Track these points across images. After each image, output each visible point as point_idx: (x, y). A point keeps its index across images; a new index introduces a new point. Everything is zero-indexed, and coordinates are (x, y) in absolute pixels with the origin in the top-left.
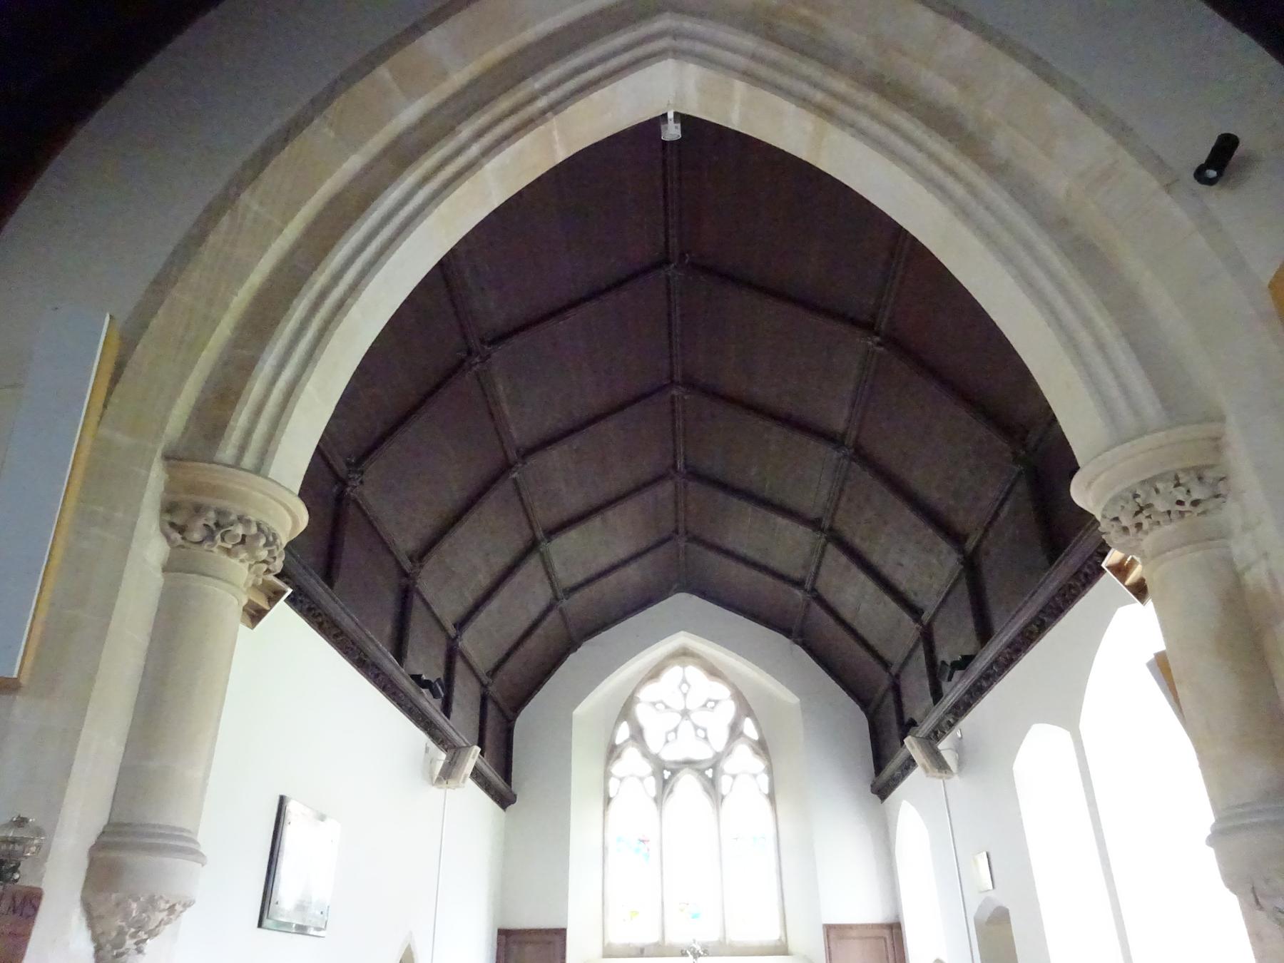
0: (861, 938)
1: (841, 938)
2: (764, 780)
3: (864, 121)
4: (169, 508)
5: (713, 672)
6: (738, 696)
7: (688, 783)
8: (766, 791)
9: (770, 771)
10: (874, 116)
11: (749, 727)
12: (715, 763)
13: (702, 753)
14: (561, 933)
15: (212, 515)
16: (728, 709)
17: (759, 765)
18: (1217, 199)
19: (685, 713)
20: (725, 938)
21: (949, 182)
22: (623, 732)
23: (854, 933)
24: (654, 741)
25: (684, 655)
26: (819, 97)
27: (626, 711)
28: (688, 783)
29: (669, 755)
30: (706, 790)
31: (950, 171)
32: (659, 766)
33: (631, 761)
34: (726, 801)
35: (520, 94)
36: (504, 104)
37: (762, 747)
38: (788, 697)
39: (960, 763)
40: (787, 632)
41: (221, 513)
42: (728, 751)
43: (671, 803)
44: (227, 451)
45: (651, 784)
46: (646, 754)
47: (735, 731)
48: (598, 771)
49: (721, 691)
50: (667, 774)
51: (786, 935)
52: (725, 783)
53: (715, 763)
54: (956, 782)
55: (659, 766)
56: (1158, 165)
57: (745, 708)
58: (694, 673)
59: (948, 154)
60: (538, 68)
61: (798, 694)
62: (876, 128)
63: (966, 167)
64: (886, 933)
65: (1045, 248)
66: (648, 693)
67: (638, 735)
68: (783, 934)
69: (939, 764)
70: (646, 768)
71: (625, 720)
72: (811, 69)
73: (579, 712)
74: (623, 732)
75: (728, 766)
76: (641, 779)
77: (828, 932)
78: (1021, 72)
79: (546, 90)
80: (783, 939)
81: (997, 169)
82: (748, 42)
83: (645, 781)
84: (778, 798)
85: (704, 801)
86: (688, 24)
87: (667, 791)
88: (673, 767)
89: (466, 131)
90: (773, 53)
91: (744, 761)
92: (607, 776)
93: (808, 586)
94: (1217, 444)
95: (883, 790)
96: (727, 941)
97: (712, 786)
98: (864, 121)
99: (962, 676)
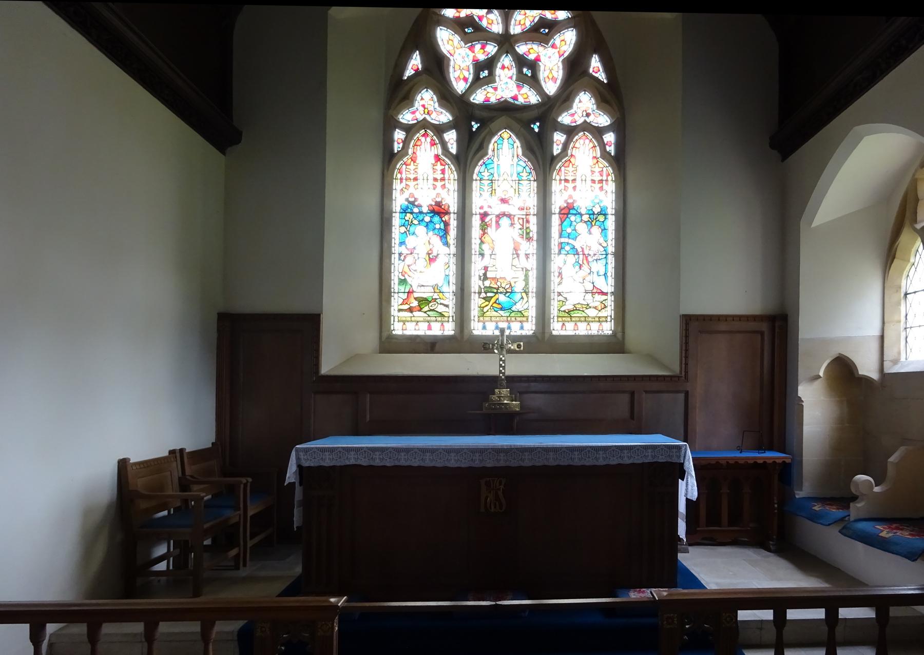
9: (619, 127)
13: (529, 97)
17: (602, 120)
20: (543, 333)
42: (564, 98)
46: (446, 96)
48: (375, 115)
50: (475, 126)
51: (623, 332)
52: (559, 138)
68: (620, 329)
74: (415, 62)
75: (565, 119)
80: (619, 335)
87: (475, 147)
88: (485, 114)
92: (391, 124)
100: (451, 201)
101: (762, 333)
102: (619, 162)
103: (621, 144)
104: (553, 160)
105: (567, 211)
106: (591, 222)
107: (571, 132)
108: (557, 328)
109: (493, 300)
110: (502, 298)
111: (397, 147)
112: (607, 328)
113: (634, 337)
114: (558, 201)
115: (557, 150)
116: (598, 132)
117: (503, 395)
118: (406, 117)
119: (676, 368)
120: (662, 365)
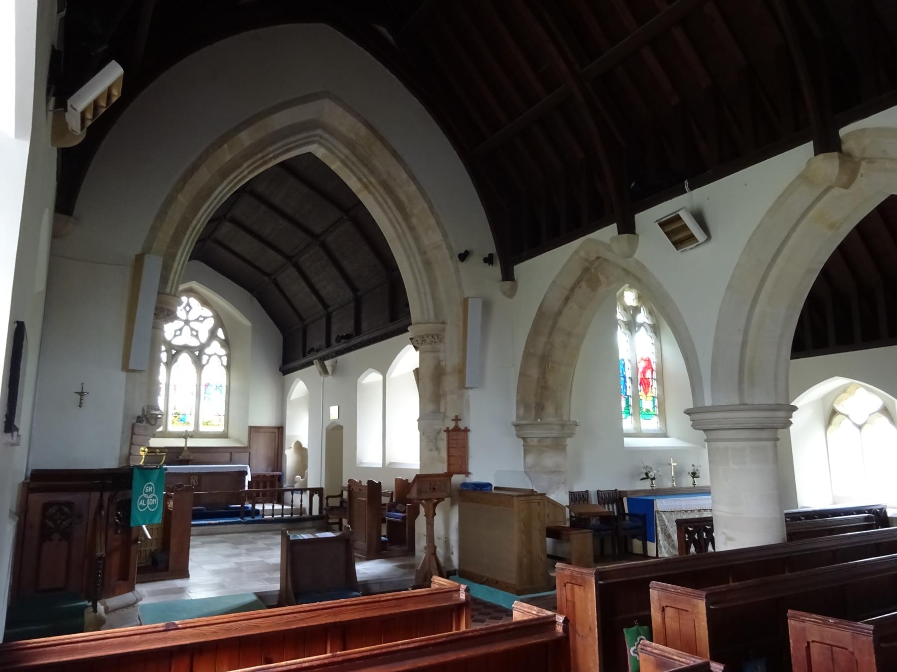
2: (225, 360)
3: (377, 195)
5: (205, 302)
7: (184, 358)
8: (225, 364)
9: (229, 356)
10: (381, 195)
11: (220, 333)
12: (202, 348)
13: (194, 343)
16: (210, 323)
17: (223, 352)
18: (462, 265)
19: (187, 322)
21: (397, 226)
23: (262, 430)
26: (365, 180)
29: (177, 342)
31: (399, 224)
34: (205, 368)
36: (260, 155)
37: (226, 344)
39: (334, 371)
40: (250, 290)
41: (168, 310)
44: (168, 290)
47: (213, 335)
49: (207, 312)
52: (205, 359)
53: (202, 348)
54: (329, 379)
56: (450, 248)
57: (220, 322)
58: (194, 302)
59: (400, 219)
60: (273, 143)
61: (251, 322)
62: (380, 199)
63: (404, 225)
64: (276, 431)
65: (418, 258)
69: (325, 371)
72: (365, 171)
75: (208, 351)
77: (250, 429)
78: (425, 205)
79: (273, 151)
81: (412, 229)
82: (346, 151)
85: (192, 368)
86: (326, 136)
88: (178, 349)
89: (245, 165)
90: (354, 159)
91: (216, 348)
94: (443, 330)
96: (167, 432)
97: (198, 362)
98: (377, 195)
99: (345, 343)
101: (275, 433)
102: (228, 368)
103: (229, 362)
104: (204, 366)
105: (207, 385)
106: (216, 389)
107: (210, 356)
109: (178, 417)
110: (181, 416)
113: (232, 432)
115: (204, 361)
116: (220, 357)
120: (243, 444)
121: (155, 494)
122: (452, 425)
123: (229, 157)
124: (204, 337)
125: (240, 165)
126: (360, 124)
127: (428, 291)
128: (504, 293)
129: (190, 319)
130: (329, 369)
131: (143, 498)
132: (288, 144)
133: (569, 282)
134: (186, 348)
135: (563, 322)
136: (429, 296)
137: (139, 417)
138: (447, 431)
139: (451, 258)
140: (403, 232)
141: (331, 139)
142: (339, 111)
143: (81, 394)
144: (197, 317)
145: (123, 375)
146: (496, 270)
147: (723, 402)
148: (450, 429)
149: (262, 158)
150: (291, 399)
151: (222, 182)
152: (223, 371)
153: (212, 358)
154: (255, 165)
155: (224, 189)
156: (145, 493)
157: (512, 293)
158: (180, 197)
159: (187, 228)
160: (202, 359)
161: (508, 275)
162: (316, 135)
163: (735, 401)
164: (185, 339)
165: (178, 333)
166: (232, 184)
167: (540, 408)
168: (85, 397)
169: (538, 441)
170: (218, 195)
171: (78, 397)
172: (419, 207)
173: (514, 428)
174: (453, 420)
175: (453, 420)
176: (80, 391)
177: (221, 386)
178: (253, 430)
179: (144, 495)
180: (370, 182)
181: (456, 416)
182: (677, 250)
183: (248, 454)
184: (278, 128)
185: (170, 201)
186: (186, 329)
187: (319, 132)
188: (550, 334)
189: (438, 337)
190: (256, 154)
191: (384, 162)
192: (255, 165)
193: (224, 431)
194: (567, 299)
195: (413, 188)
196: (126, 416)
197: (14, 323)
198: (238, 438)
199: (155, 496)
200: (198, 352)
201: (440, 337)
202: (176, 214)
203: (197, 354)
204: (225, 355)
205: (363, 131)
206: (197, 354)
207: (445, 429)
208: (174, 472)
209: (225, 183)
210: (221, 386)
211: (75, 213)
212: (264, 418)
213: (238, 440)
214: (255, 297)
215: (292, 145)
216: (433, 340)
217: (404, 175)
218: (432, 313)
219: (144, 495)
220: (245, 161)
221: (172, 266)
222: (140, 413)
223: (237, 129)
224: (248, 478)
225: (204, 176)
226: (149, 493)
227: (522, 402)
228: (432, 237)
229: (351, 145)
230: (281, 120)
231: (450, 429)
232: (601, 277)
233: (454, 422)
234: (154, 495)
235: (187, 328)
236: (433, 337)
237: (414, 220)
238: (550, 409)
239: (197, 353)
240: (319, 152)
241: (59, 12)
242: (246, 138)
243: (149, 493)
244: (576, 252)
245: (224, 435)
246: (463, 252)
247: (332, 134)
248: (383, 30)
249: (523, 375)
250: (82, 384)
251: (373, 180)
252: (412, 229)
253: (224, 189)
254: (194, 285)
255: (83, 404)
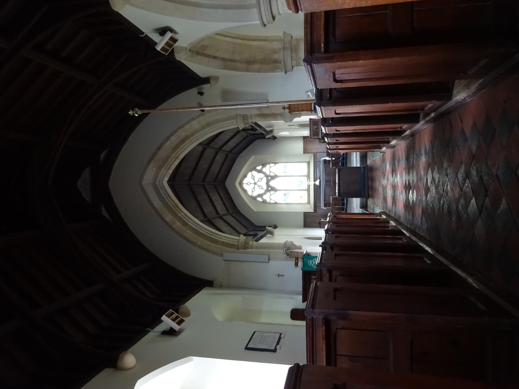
0: (306, 145)
1: (306, 150)
2: (271, 165)
3: (180, 152)
4: (244, 249)
5: (245, 176)
6: (251, 170)
7: (272, 183)
8: (274, 164)
9: (269, 164)
10: (179, 151)
11: (259, 168)
12: (267, 176)
13: (265, 180)
14: (304, 213)
15: (245, 244)
16: (254, 173)
17: (268, 166)
19: (255, 184)
21: (193, 141)
22: (259, 199)
23: (305, 147)
24: (262, 192)
25: (241, 184)
26: (174, 159)
27: (254, 198)
28: (272, 183)
29: (265, 187)
30: (274, 179)
31: (191, 141)
32: (267, 191)
33: (266, 197)
34: (276, 174)
35: (172, 207)
36: (174, 209)
37: (264, 165)
38: (252, 158)
40: (237, 158)
41: (245, 243)
42: (265, 174)
43: (277, 187)
44: (236, 244)
45: (272, 192)
46: (265, 193)
47: (260, 171)
49: (250, 175)
50: (270, 189)
52: (272, 174)
53: (267, 176)
55: (267, 191)
57: (254, 169)
58: (245, 181)
60: (167, 204)
61: (252, 156)
62: (181, 151)
63: (191, 138)
64: (305, 140)
65: (206, 130)
66: (250, 193)
67: (260, 196)
70: (268, 194)
71: (256, 199)
72: (170, 160)
73: (255, 210)
75: (268, 173)
76: (271, 195)
78: (180, 131)
79: (171, 203)
81: (193, 134)
82: (163, 169)
83: (271, 194)
84: (276, 162)
86: (158, 179)
87: (274, 189)
89: (180, 215)
90: (166, 166)
91: (266, 169)
92: (270, 203)
93: (228, 153)
94: (240, 115)
95: (274, 138)
97: (273, 177)
98: (180, 152)
100: (284, 192)
102: (275, 163)
103: (272, 163)
104: (275, 175)
107: (270, 172)
108: (306, 173)
111: (274, 202)
112: (305, 165)
113: (307, 160)
114: (284, 174)
115: (274, 175)
117: (317, 183)
118: (268, 201)
119: (312, 155)
121: (313, 260)
122: (287, 111)
123: (178, 223)
124: (261, 175)
125: (180, 217)
126: (149, 167)
127: (221, 123)
128: (217, 82)
129: (254, 182)
130: (271, 129)
131: (314, 265)
132: (166, 196)
133: (206, 60)
134: (267, 183)
135: (227, 56)
136: (224, 123)
137: (287, 255)
138: (290, 112)
139: (203, 115)
140: (195, 138)
141: (159, 177)
142: (146, 177)
143: (279, 275)
144: (252, 179)
145: (271, 262)
146: (206, 87)
147: (257, 16)
148: (289, 111)
149: (175, 208)
150: (289, 135)
151: (189, 225)
152: (277, 165)
153: (271, 171)
154: (179, 211)
155: (192, 223)
156: (312, 264)
157: (217, 78)
158: (199, 243)
159: (211, 238)
160: (272, 176)
161: (207, 80)
162: (159, 183)
163: (255, 11)
164: (263, 183)
165: (260, 180)
166: (188, 219)
167: (275, 61)
168: (280, 274)
169: (294, 60)
170: (195, 226)
171: (280, 277)
172: (181, 133)
173: (287, 73)
174: (285, 110)
175: (285, 110)
176: (277, 276)
177: (285, 166)
178: (305, 151)
179: (313, 265)
180: (174, 156)
181: (283, 108)
182: (178, 40)
183: (317, 153)
184: (161, 203)
185: (200, 247)
186: (258, 183)
187: (157, 183)
188: (235, 61)
189: (244, 117)
190: (174, 211)
191: (163, 153)
192: (179, 211)
193: (307, 163)
194: (215, 57)
195: (173, 138)
196: (286, 260)
197: (245, 351)
198: (310, 157)
199: (314, 260)
200: (269, 178)
201: (244, 116)
202: (207, 243)
203: (270, 178)
204: (269, 165)
205: (152, 165)
206: (270, 178)
207: (289, 113)
208: (323, 193)
209: (189, 223)
210: (285, 166)
211: (212, 280)
212: (300, 146)
213: (311, 158)
214: (239, 155)
215: (166, 195)
216: (246, 120)
217: (168, 143)
218: (233, 121)
219: (313, 265)
220: (178, 215)
221: (227, 243)
222: (286, 255)
223: (166, 222)
224: (327, 158)
225: (188, 233)
226: (312, 263)
227: (273, 70)
228: (195, 125)
229: (160, 167)
230: (157, 203)
231: (289, 111)
232: (200, 45)
233: (286, 109)
234: (313, 261)
235: (258, 183)
236: (244, 120)
237: (188, 133)
238: (276, 56)
239: (270, 178)
240: (166, 179)
241: (150, 331)
242: (169, 218)
243: (312, 263)
244: (189, 61)
245: (309, 163)
246: (199, 95)
247: (157, 177)
248: (102, 156)
249: (259, 71)
250: (275, 275)
251: (173, 156)
252: (193, 134)
253: (192, 223)
254: (237, 184)
255: (283, 274)
